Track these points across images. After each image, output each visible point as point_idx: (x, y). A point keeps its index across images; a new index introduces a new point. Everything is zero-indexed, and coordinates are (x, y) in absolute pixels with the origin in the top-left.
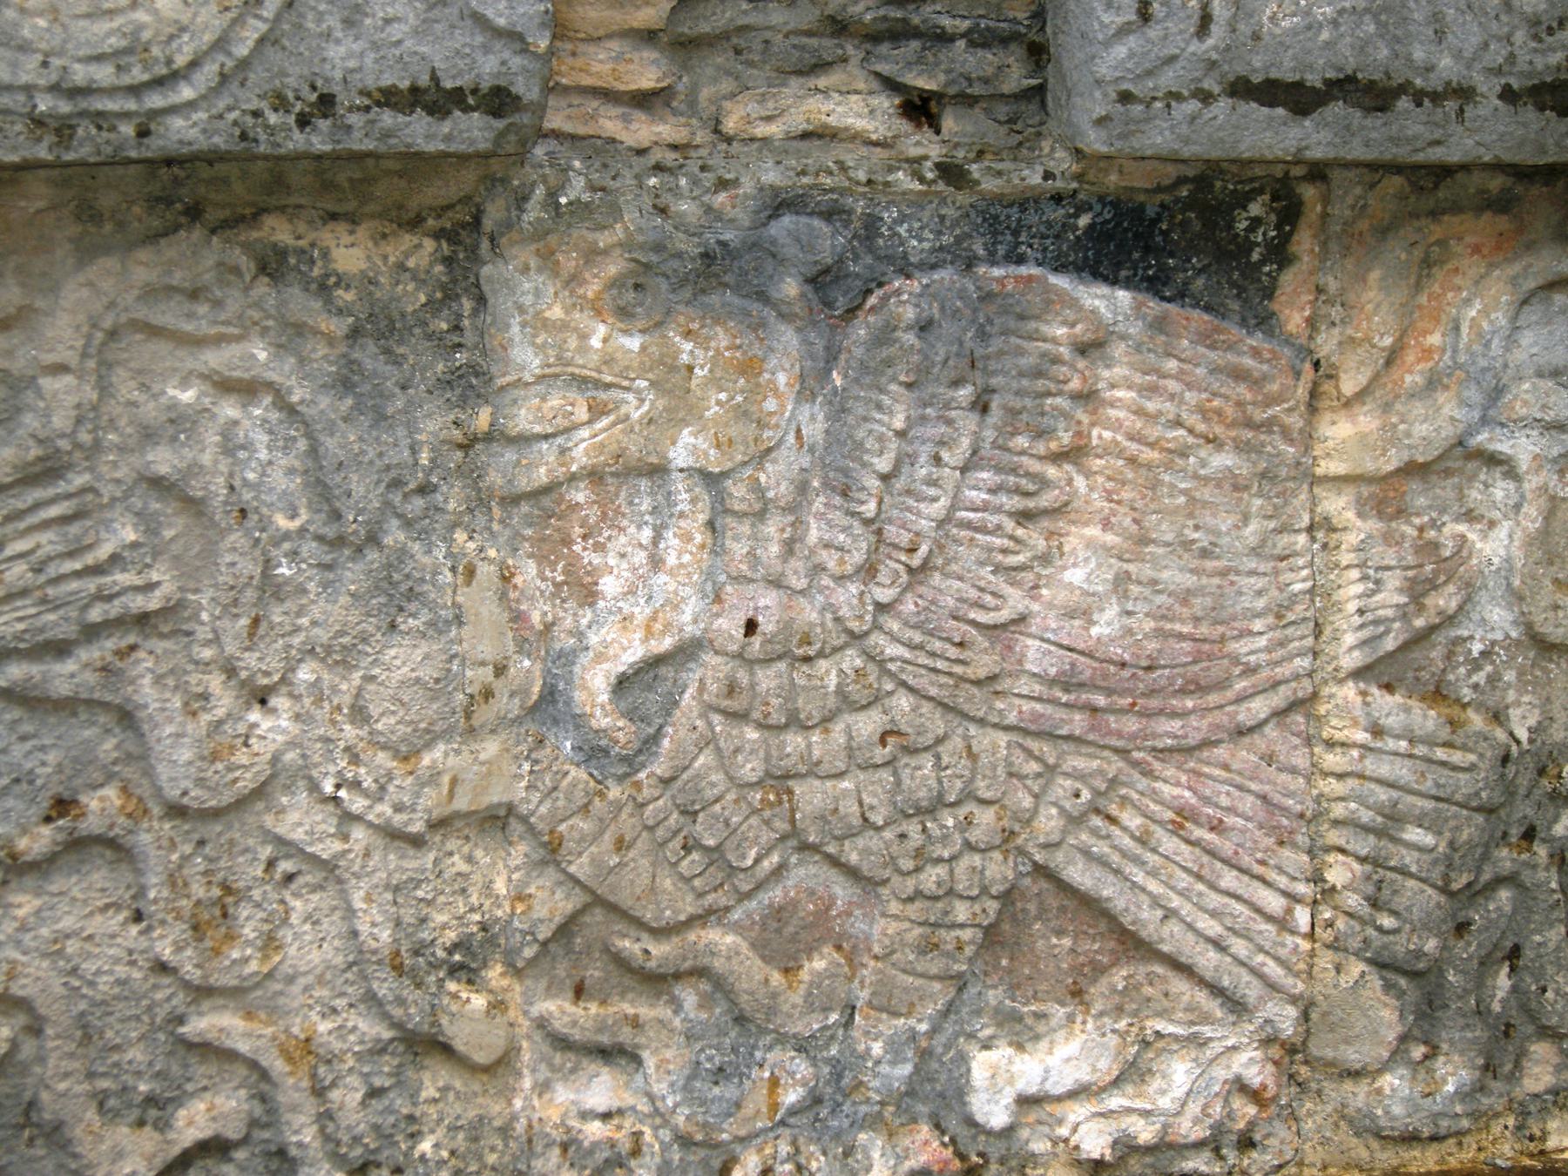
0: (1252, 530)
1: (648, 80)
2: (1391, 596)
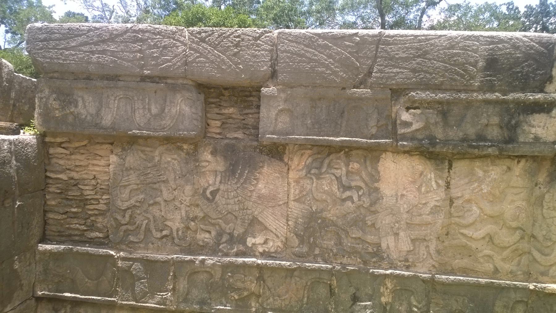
0: (280, 183)
1: (218, 131)
2: (297, 192)
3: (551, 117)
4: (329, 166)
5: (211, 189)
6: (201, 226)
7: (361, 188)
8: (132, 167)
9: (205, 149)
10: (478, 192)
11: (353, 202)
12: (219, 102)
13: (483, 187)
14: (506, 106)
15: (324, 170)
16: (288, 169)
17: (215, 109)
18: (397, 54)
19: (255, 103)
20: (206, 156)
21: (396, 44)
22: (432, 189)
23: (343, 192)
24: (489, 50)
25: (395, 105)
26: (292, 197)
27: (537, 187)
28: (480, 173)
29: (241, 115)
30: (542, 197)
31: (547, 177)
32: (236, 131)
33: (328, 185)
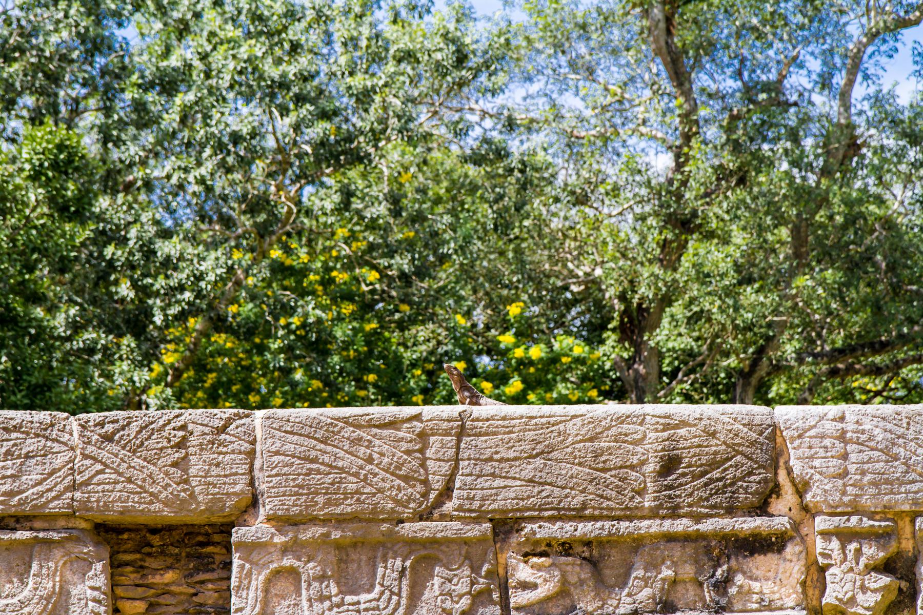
3: (785, 560)
12: (141, 560)
14: (704, 543)
17: (133, 576)
18: (497, 453)
19: (218, 558)
21: (494, 434)
25: (502, 549)
29: (188, 585)
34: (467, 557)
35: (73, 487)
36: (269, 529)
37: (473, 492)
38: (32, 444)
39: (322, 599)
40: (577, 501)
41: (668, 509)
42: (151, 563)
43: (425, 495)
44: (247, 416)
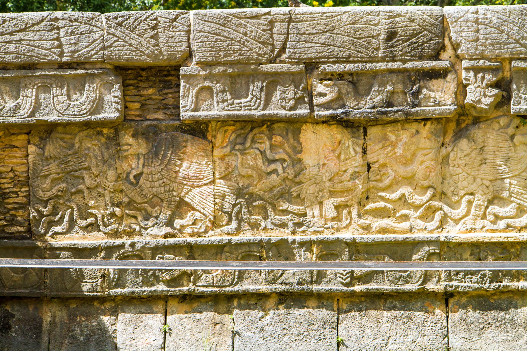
2: (223, 169)
3: (447, 82)
4: (253, 141)
5: (134, 172)
6: (126, 211)
7: (285, 160)
8: (52, 155)
9: (126, 132)
10: (392, 156)
11: (278, 175)
12: (138, 83)
13: (396, 150)
14: (408, 74)
15: (248, 145)
16: (213, 147)
17: (134, 91)
18: (307, 30)
19: (174, 82)
20: (127, 139)
21: (306, 21)
22: (351, 156)
23: (268, 166)
24: (389, 24)
25: (310, 78)
26: (217, 176)
27: (444, 147)
28: (392, 137)
29: (160, 95)
30: (448, 155)
31: (452, 137)
32: (157, 112)
33: (252, 159)
34: (293, 81)
35: (104, 48)
36: (198, 68)
37: (296, 50)
38: (83, 28)
39: (223, 101)
40: (346, 53)
41: (390, 57)
42: (141, 84)
43: (272, 51)
44: (186, 13)
